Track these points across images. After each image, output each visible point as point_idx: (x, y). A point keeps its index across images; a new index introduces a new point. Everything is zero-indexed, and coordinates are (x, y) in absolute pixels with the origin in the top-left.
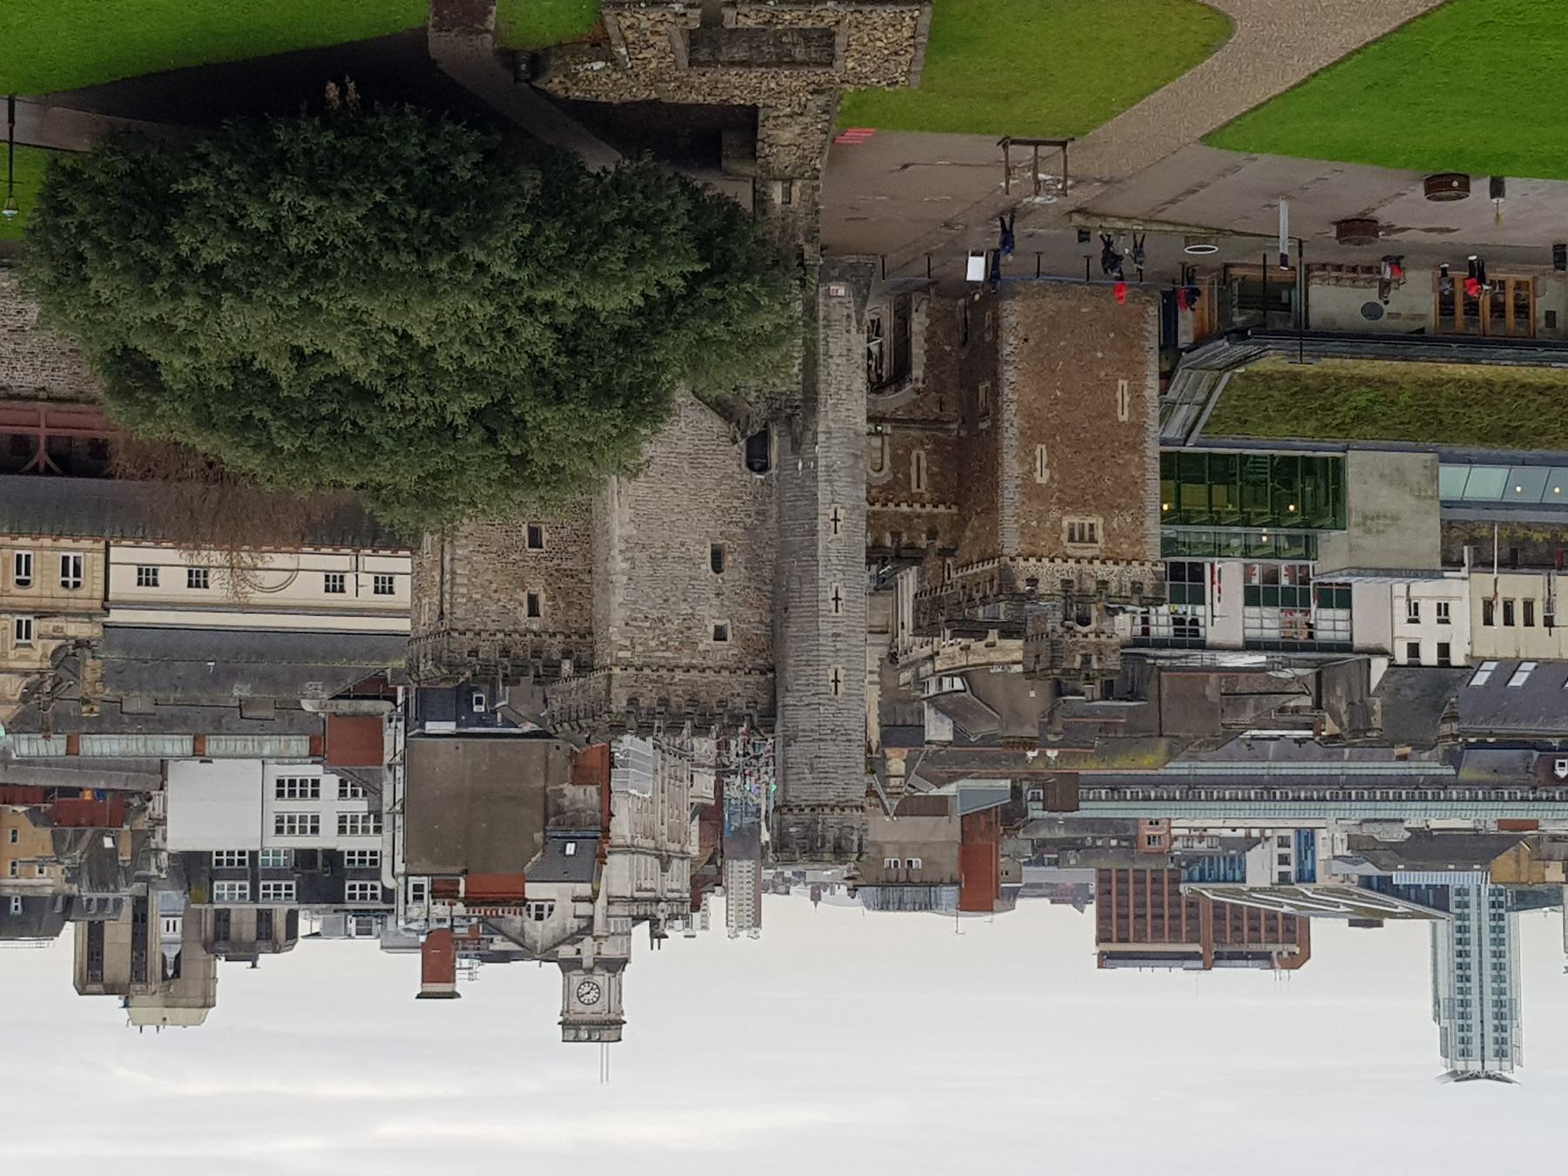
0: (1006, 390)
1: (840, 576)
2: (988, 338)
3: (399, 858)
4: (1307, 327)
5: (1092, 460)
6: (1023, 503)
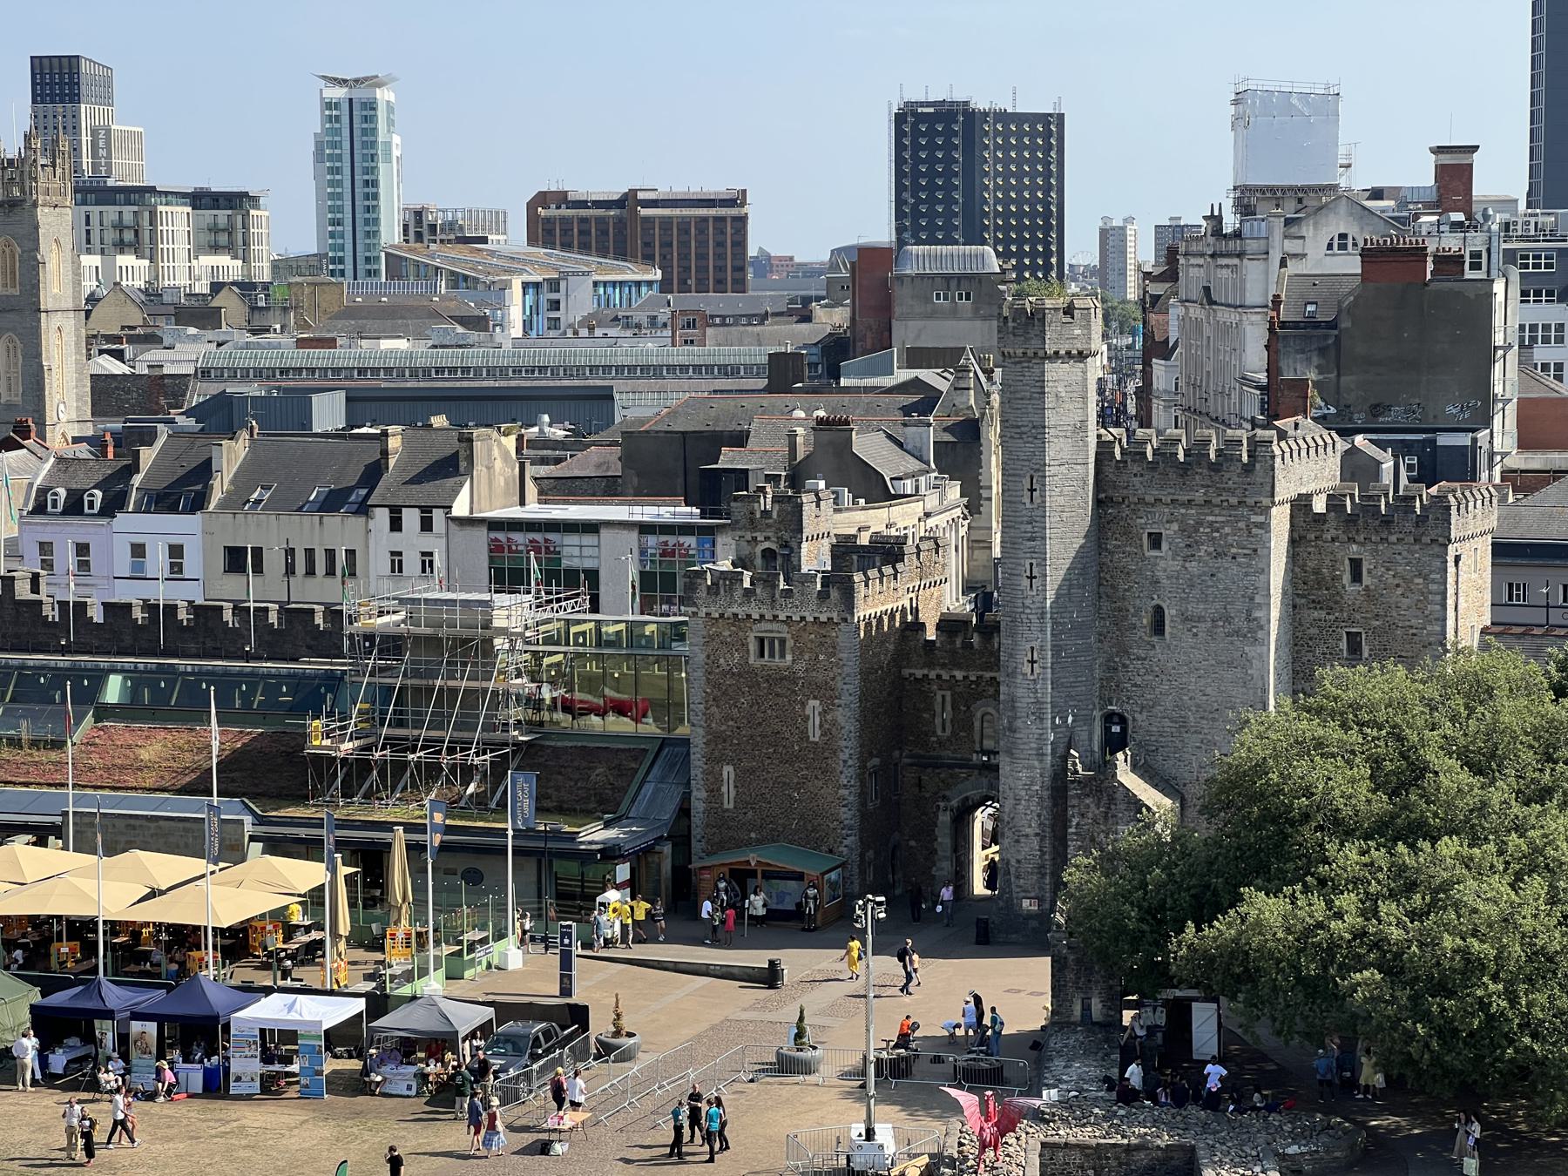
0: (851, 798)
1: (1028, 602)
2: (870, 854)
3: (1500, 298)
4: (539, 862)
5: (760, 724)
6: (833, 679)
